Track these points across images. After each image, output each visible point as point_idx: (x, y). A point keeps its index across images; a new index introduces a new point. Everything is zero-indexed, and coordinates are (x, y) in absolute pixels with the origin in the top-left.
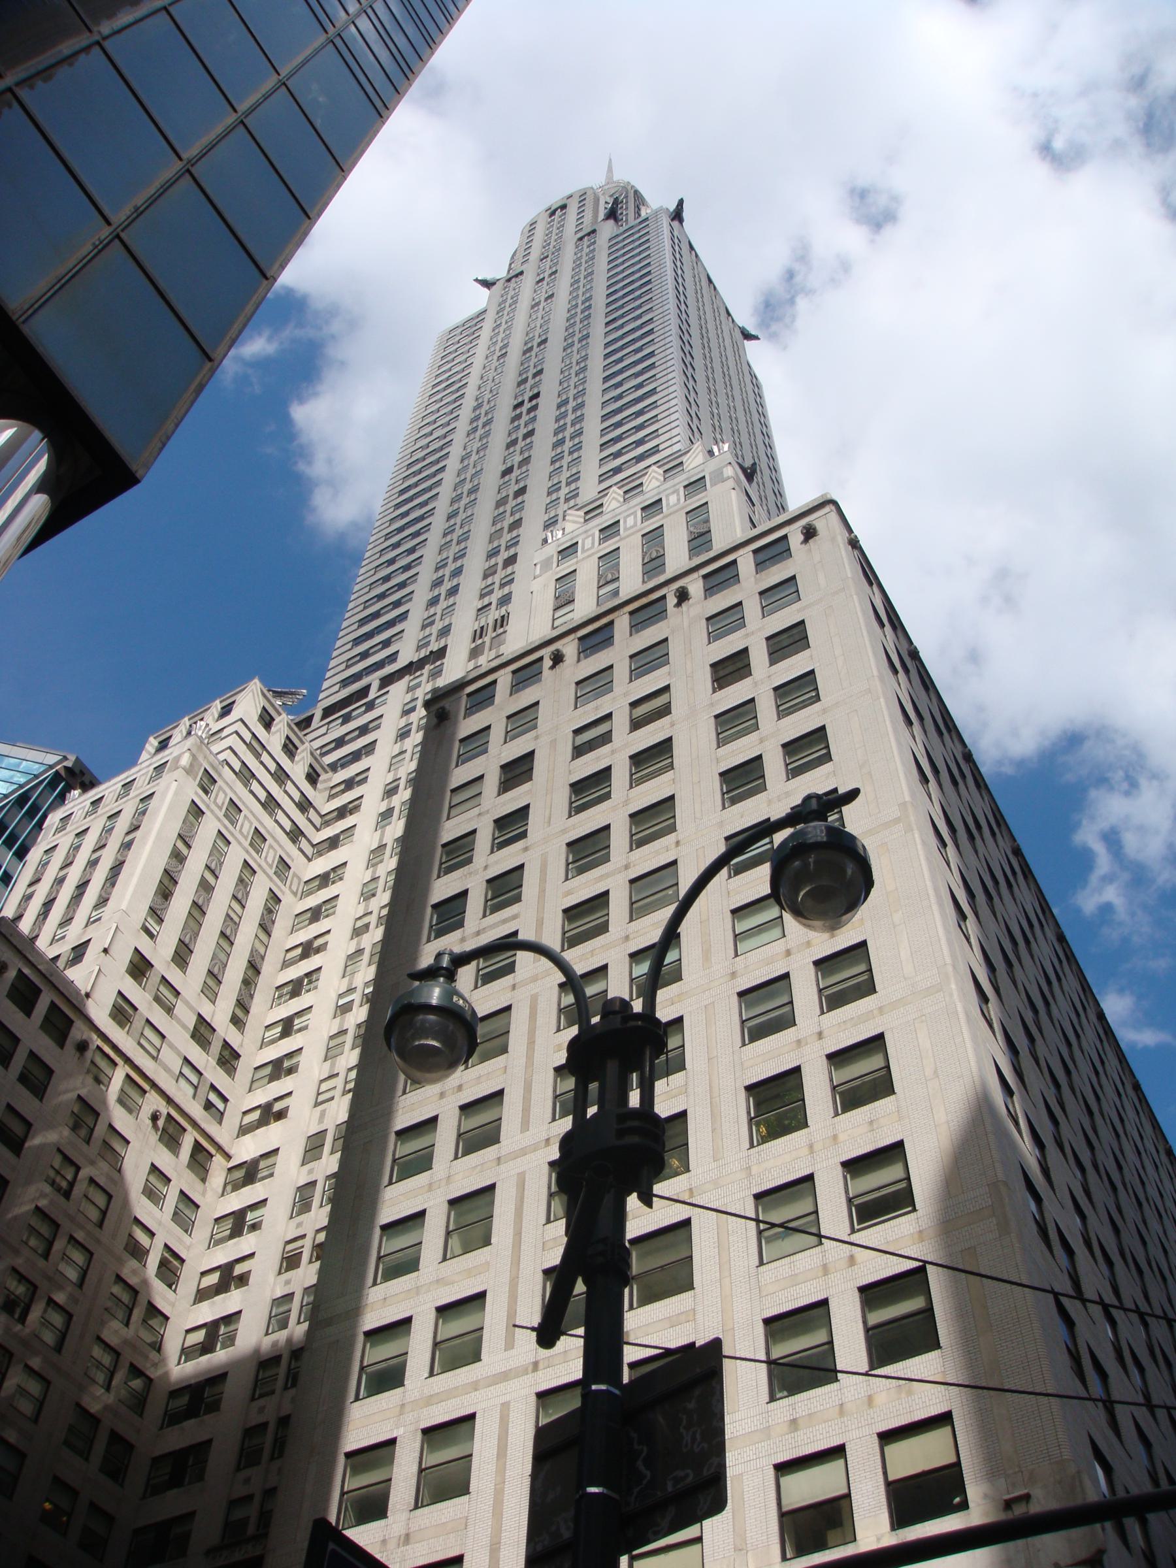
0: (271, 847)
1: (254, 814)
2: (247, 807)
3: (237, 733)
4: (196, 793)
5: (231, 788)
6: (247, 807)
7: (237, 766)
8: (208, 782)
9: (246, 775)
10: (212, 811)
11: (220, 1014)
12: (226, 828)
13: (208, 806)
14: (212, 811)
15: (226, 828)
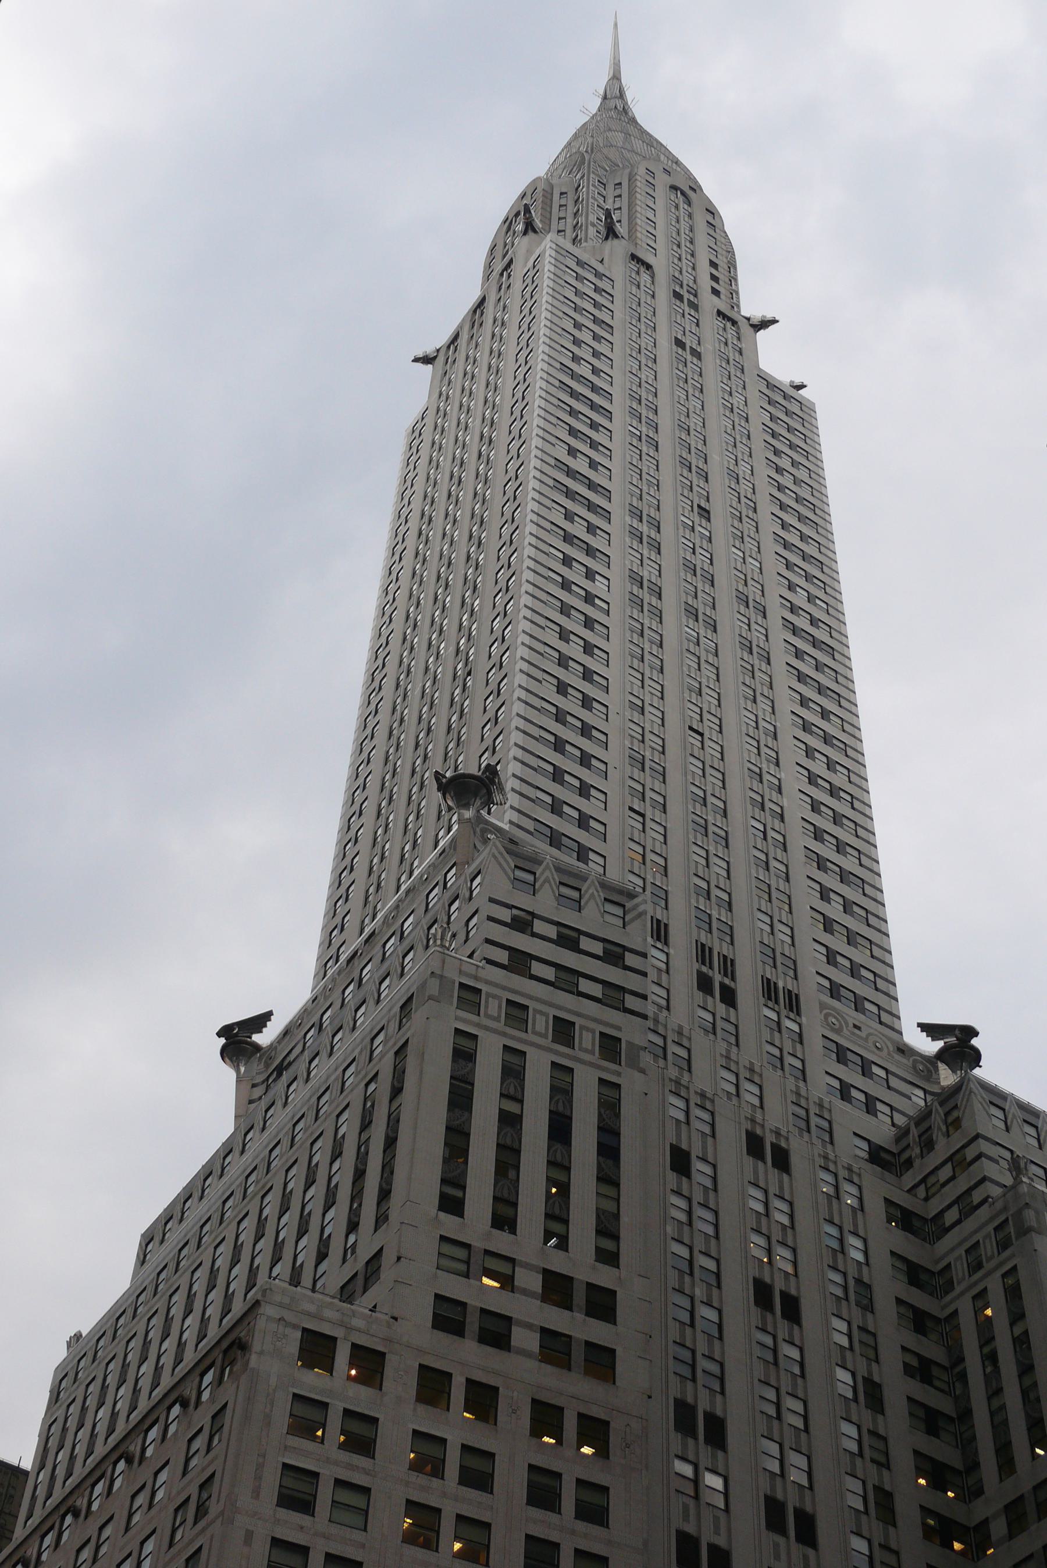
0: (582, 1027)
1: (545, 1001)
2: (531, 998)
3: (490, 919)
4: (457, 1018)
5: (504, 988)
6: (531, 998)
7: (503, 957)
8: (470, 996)
9: (519, 962)
10: (487, 1028)
11: (579, 1262)
12: (513, 1038)
13: (478, 1025)
14: (487, 1028)
15: (513, 1038)
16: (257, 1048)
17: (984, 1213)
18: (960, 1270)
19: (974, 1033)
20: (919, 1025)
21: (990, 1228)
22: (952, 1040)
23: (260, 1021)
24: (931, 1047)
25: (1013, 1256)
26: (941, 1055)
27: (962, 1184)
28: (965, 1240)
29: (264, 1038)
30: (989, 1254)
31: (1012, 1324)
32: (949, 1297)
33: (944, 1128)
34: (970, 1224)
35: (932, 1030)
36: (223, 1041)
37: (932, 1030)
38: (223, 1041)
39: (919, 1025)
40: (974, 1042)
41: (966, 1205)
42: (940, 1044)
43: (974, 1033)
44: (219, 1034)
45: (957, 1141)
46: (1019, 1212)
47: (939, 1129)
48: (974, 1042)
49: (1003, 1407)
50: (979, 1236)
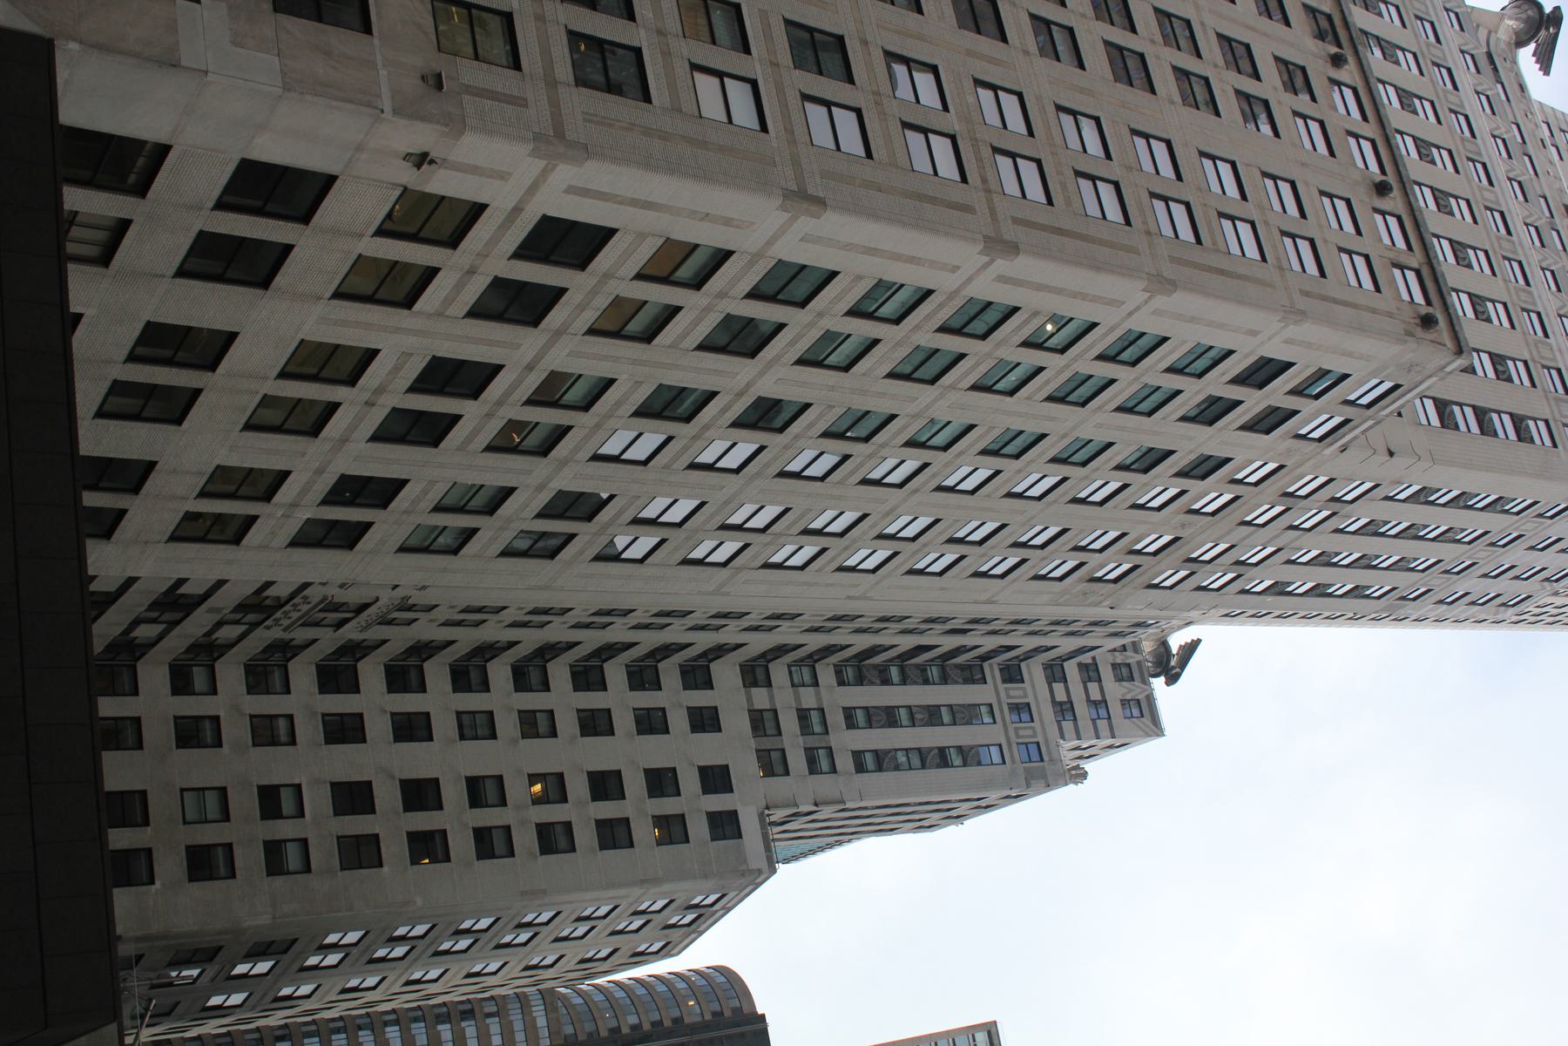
16: (1520, 44)
17: (1053, 730)
18: (1016, 693)
19: (1168, 684)
20: (1199, 641)
21: (1040, 739)
22: (1173, 663)
23: (1545, 60)
24: (1176, 641)
25: (1013, 762)
26: (1164, 644)
27: (1081, 708)
28: (1038, 707)
29: (1526, 57)
30: (1021, 733)
31: (960, 749)
32: (997, 673)
33: (1128, 697)
34: (1048, 712)
35: (1190, 649)
36: (1548, 9)
37: (1190, 649)
38: (1548, 9)
39: (1199, 641)
40: (1162, 679)
41: (1064, 709)
42: (1174, 651)
43: (1168, 684)
44: (1557, 9)
45: (1115, 708)
46: (1044, 777)
47: (1130, 691)
48: (1162, 679)
49: (886, 681)
50: (1037, 724)
